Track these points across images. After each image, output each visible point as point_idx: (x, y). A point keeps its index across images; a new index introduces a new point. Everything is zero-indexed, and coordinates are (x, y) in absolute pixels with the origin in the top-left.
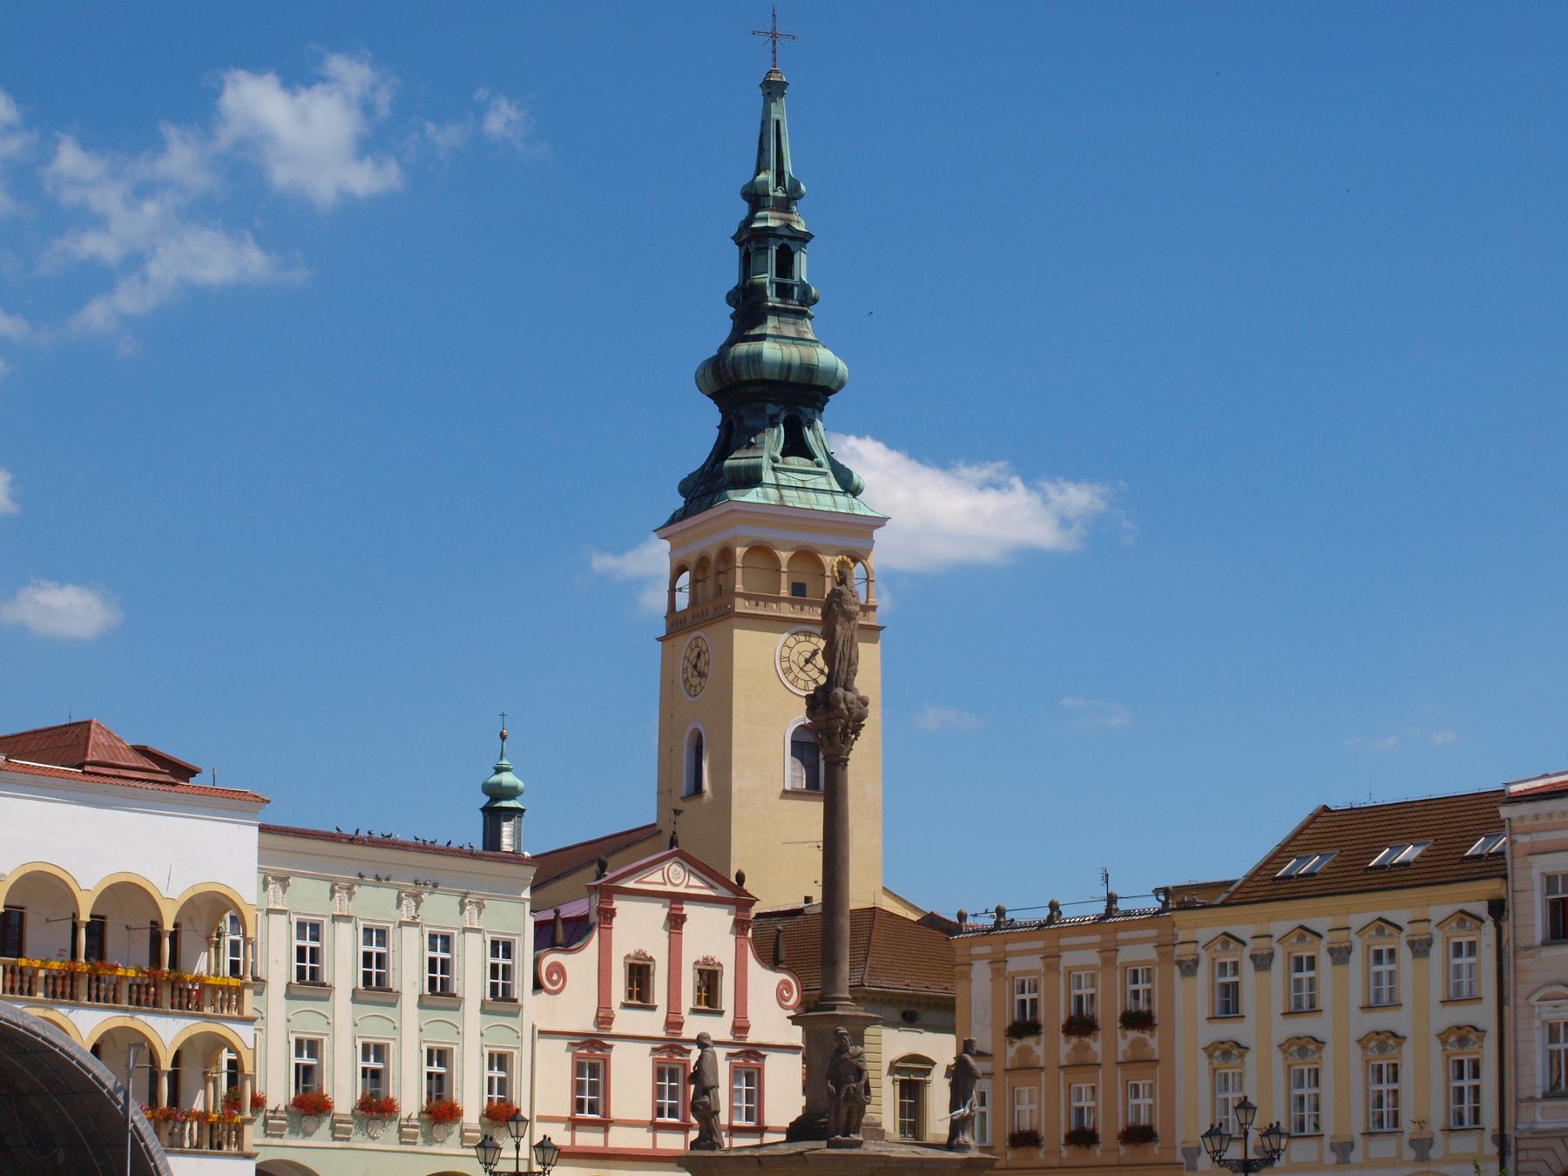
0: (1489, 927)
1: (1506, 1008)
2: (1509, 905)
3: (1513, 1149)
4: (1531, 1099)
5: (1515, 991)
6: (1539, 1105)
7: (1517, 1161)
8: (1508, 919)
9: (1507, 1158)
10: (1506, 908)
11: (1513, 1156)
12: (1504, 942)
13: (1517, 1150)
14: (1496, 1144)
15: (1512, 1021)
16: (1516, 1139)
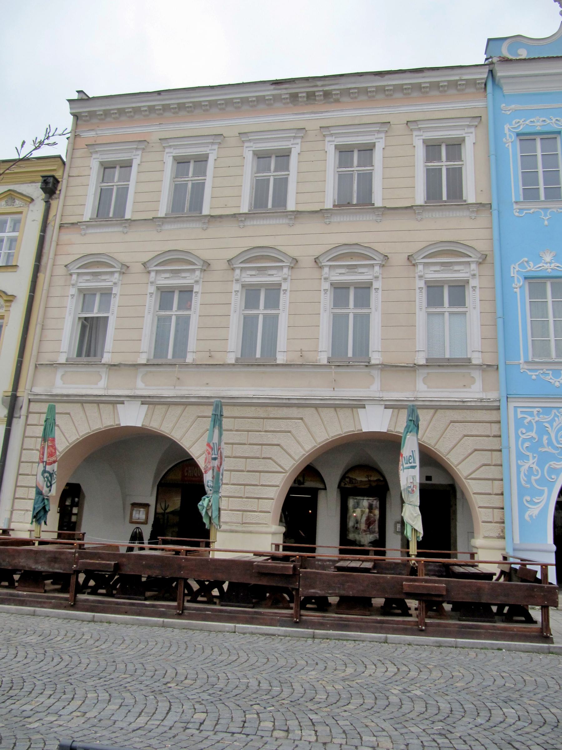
0: (39, 207)
1: (41, 276)
2: (62, 186)
3: (24, 411)
4: (53, 365)
5: (54, 260)
6: (60, 372)
7: (26, 424)
8: (59, 198)
9: (15, 421)
10: (59, 188)
11: (23, 418)
12: (51, 217)
13: (29, 412)
14: (5, 406)
15: (46, 287)
16: (30, 401)
